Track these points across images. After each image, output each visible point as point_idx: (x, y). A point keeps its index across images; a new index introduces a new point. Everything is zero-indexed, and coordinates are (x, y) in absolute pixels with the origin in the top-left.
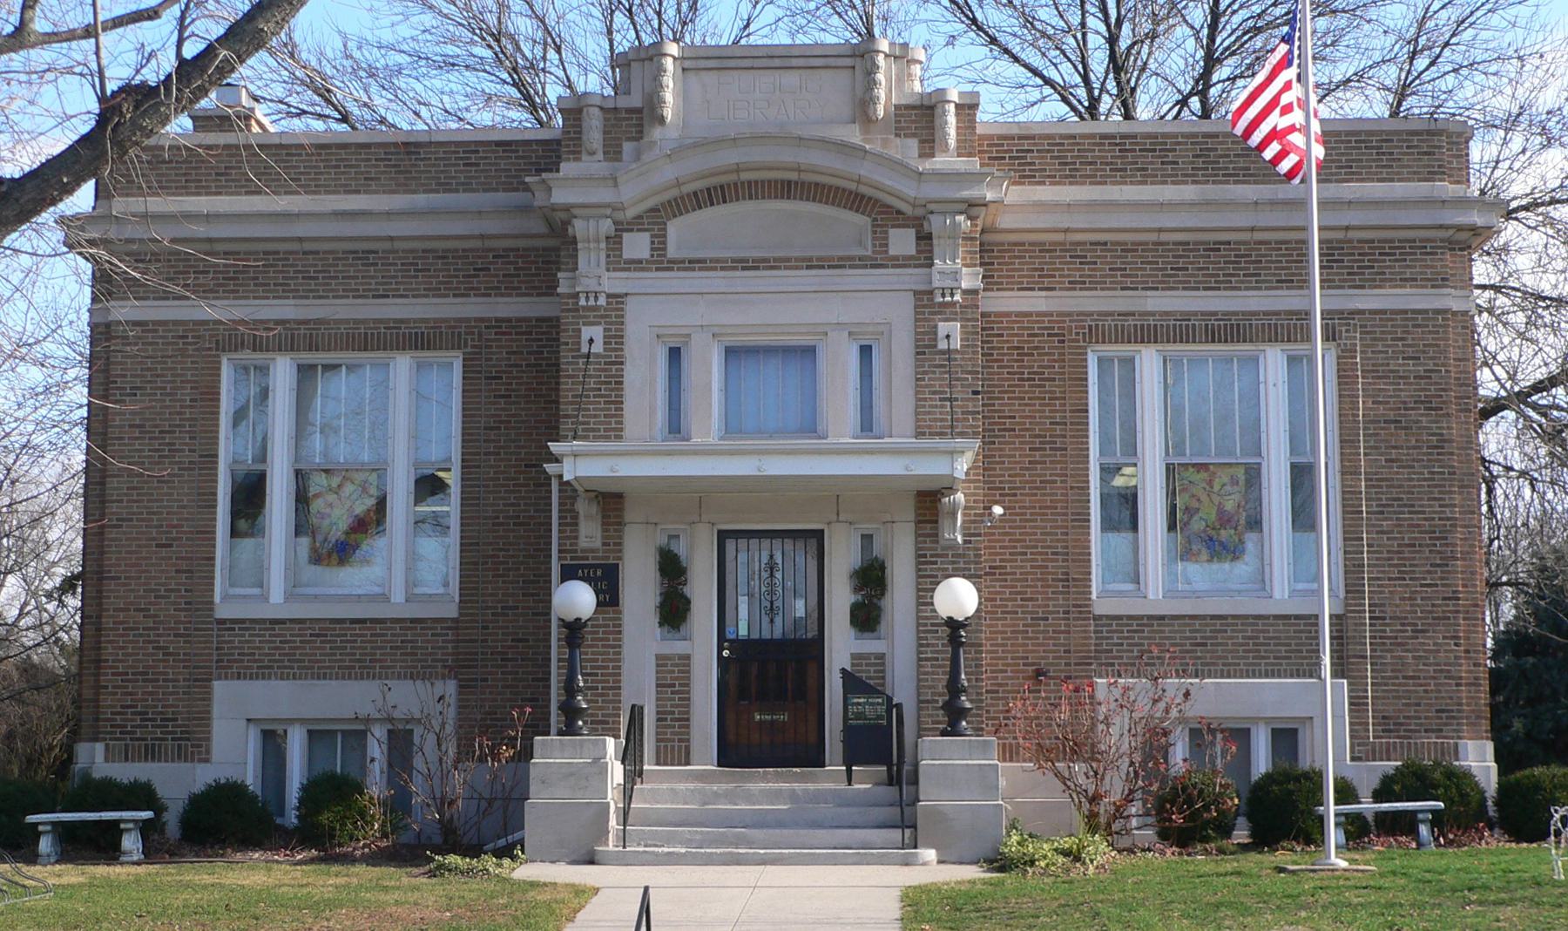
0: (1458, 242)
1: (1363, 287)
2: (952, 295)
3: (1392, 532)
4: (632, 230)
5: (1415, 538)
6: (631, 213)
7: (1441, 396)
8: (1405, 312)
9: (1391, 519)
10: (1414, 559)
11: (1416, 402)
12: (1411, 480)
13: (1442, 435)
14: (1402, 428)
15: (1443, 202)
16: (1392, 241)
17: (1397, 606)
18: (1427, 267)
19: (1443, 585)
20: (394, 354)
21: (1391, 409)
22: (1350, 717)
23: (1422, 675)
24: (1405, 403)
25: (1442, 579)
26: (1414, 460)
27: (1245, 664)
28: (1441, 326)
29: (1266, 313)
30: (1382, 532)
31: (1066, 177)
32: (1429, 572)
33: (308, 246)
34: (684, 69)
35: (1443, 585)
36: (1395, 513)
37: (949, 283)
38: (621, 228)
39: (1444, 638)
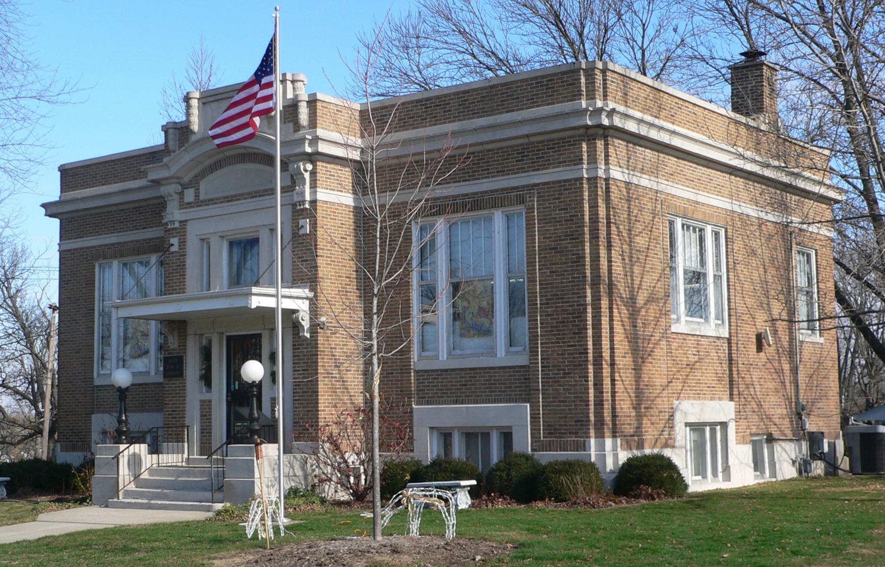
0: (592, 135)
1: (538, 170)
2: (304, 205)
3: (553, 315)
4: (188, 188)
5: (565, 318)
6: (186, 179)
7: (578, 231)
8: (560, 182)
9: (552, 307)
10: (564, 330)
11: (565, 236)
12: (562, 283)
13: (579, 254)
14: (558, 252)
15: (567, 113)
16: (553, 140)
17: (555, 359)
18: (571, 153)
19: (579, 345)
20: (150, 255)
21: (553, 241)
22: (531, 426)
23: (568, 400)
24: (559, 237)
25: (578, 341)
26: (564, 271)
27: (485, 396)
28: (578, 188)
29: (492, 191)
30: (549, 315)
31: (401, 127)
32: (572, 338)
33: (121, 207)
34: (204, 104)
35: (579, 345)
36: (554, 303)
37: (300, 199)
38: (184, 187)
39: (579, 377)
